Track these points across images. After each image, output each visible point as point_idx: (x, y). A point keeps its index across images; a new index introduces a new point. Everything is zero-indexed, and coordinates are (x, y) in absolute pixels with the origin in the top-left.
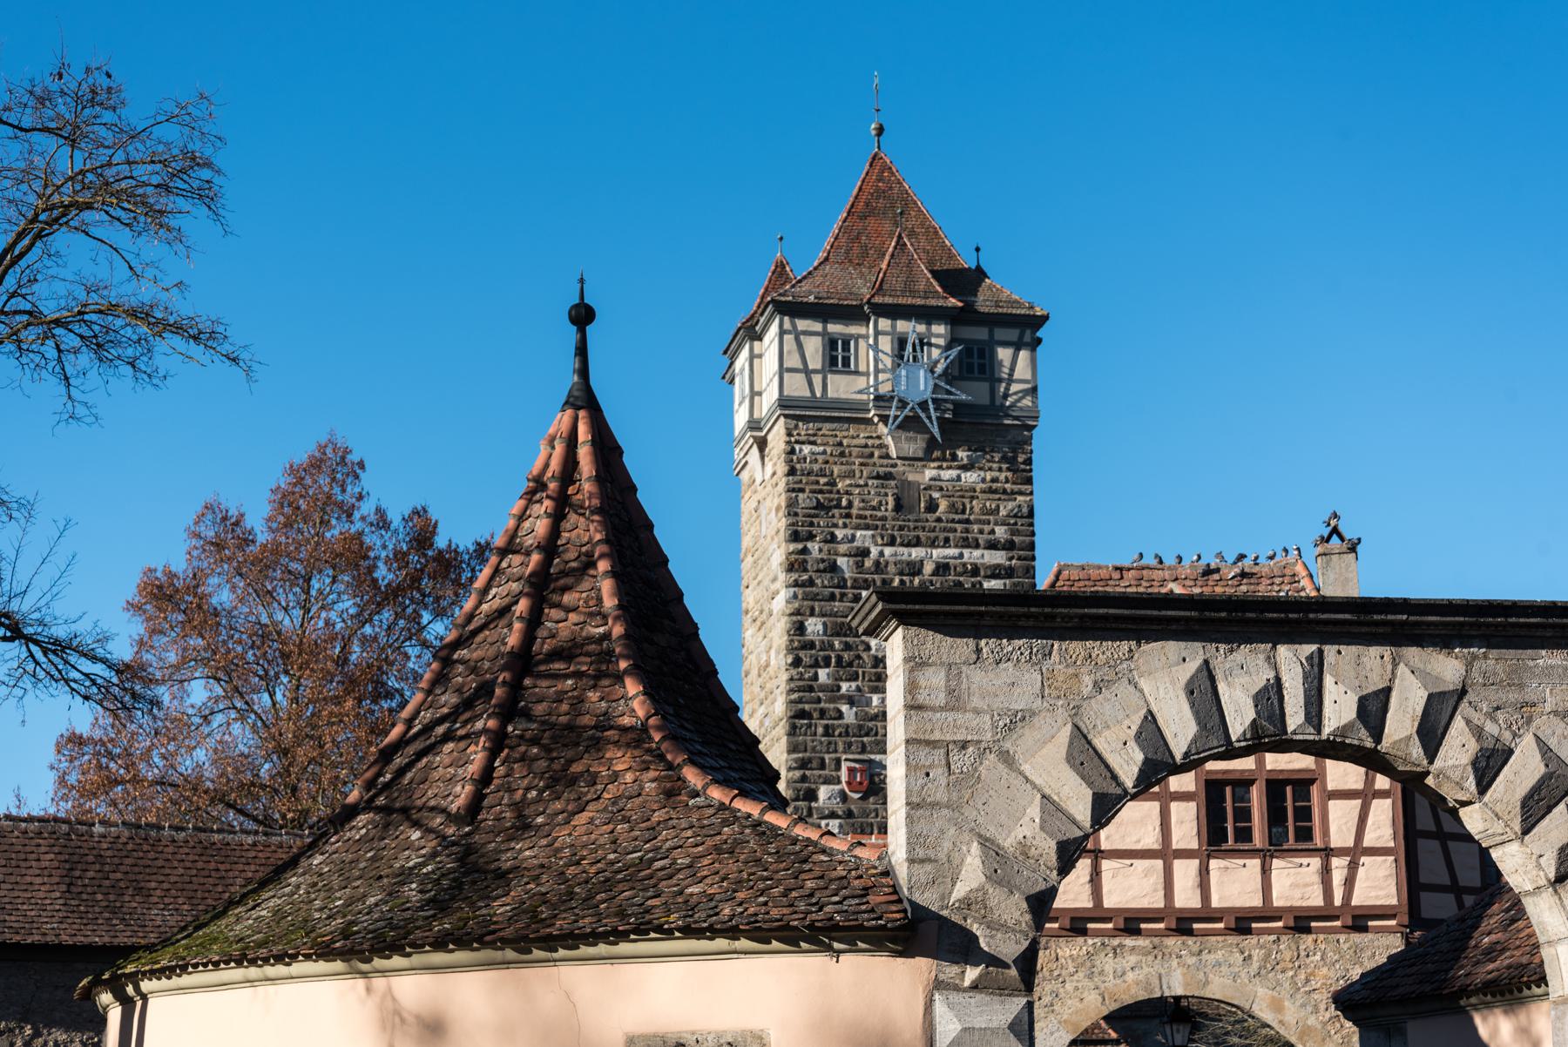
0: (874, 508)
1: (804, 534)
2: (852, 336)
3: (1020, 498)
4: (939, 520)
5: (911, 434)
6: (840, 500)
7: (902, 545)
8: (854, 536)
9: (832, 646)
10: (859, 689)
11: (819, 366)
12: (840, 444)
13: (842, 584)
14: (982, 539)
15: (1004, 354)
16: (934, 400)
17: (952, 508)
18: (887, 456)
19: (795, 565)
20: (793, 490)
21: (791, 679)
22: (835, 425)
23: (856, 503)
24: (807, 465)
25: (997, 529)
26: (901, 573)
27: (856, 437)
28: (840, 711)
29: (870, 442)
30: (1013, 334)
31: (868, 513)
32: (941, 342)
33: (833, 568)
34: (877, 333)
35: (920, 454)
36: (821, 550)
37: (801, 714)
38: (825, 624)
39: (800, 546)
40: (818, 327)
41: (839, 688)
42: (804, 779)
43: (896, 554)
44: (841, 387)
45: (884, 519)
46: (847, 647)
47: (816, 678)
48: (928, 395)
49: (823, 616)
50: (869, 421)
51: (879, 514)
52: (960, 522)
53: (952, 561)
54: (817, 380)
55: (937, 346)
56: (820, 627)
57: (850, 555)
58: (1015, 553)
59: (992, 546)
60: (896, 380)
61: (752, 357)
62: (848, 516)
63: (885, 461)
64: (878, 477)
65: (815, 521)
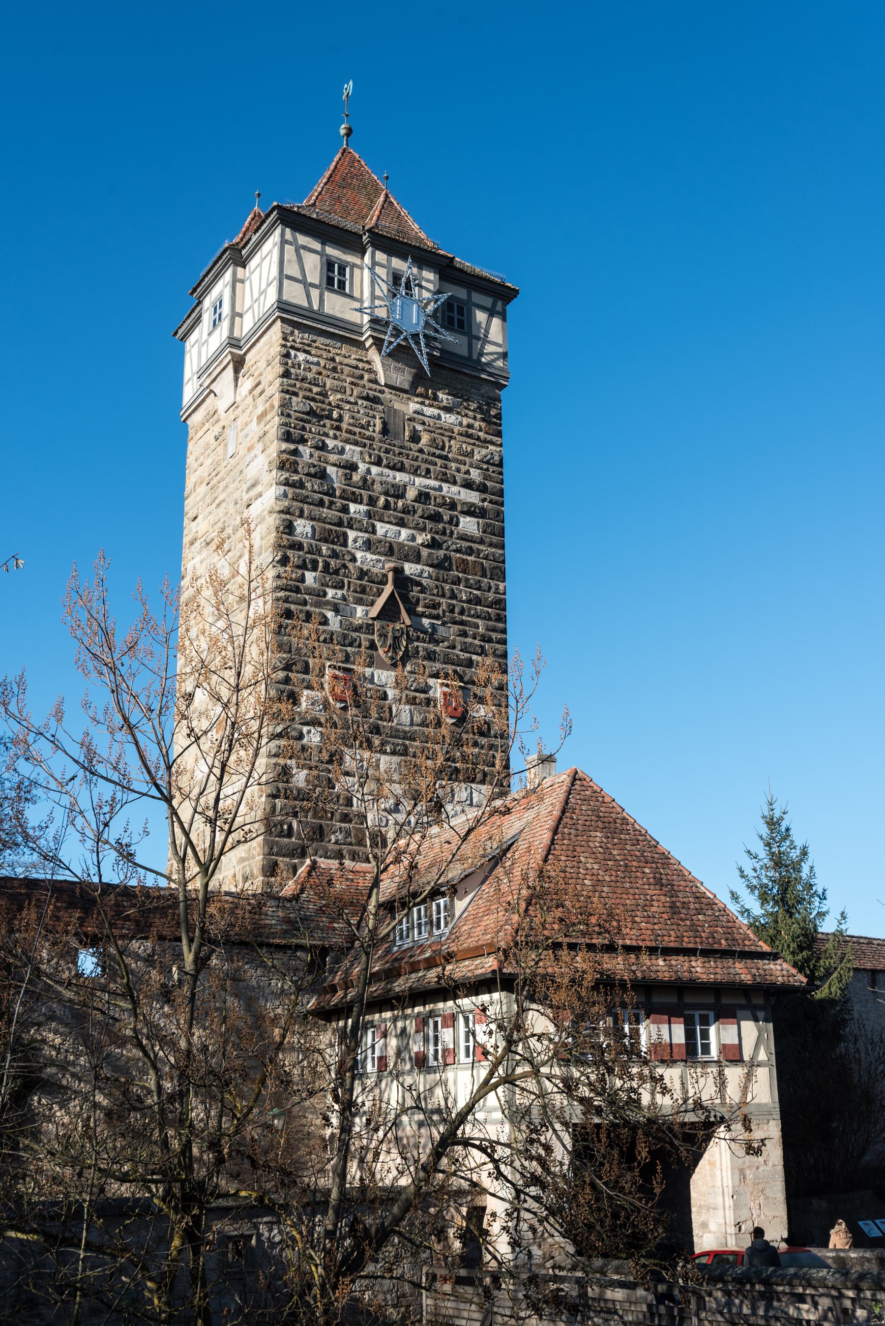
0: (362, 427)
1: (296, 433)
2: (348, 263)
3: (491, 447)
4: (421, 451)
5: (400, 365)
6: (331, 411)
7: (388, 466)
8: (343, 449)
9: (319, 552)
10: (344, 598)
11: (317, 282)
12: (333, 360)
13: (331, 493)
14: (459, 477)
15: (481, 316)
16: (425, 336)
17: (433, 442)
18: (376, 382)
19: (287, 463)
20: (287, 392)
21: (279, 577)
22: (328, 341)
23: (346, 418)
24: (301, 372)
25: (472, 470)
26: (386, 494)
27: (347, 355)
28: (325, 617)
29: (361, 365)
30: (488, 301)
31: (357, 430)
32: (431, 286)
33: (322, 475)
34: (374, 264)
35: (406, 387)
36: (311, 456)
37: (288, 614)
38: (313, 527)
39: (292, 447)
40: (317, 246)
41: (325, 594)
42: (287, 681)
43: (381, 474)
44: (335, 306)
45: (371, 438)
46: (335, 555)
47: (302, 579)
48: (420, 329)
49: (312, 519)
50: (360, 345)
51: (367, 433)
52: (440, 457)
53: (432, 492)
54: (315, 293)
55: (428, 290)
56: (309, 530)
57: (339, 466)
58: (488, 497)
59: (468, 485)
60: (391, 310)
61: (235, 281)
62: (338, 428)
63: (374, 386)
64: (367, 398)
65: (307, 426)
